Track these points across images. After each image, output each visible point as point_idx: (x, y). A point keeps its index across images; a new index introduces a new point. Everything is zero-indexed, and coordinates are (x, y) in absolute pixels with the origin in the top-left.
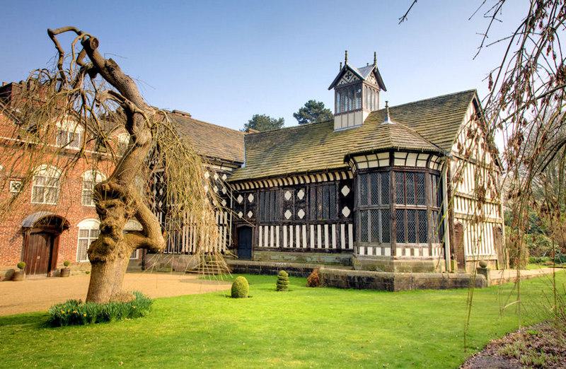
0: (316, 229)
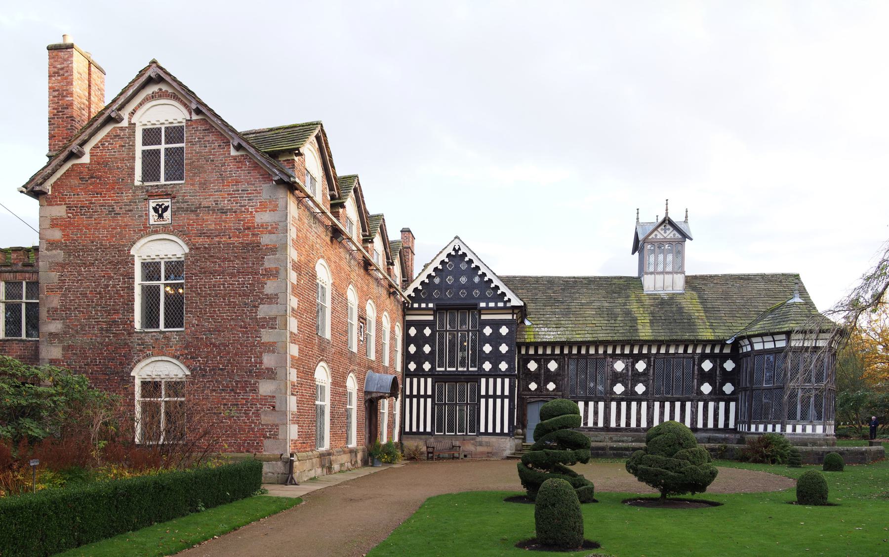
0: (662, 407)
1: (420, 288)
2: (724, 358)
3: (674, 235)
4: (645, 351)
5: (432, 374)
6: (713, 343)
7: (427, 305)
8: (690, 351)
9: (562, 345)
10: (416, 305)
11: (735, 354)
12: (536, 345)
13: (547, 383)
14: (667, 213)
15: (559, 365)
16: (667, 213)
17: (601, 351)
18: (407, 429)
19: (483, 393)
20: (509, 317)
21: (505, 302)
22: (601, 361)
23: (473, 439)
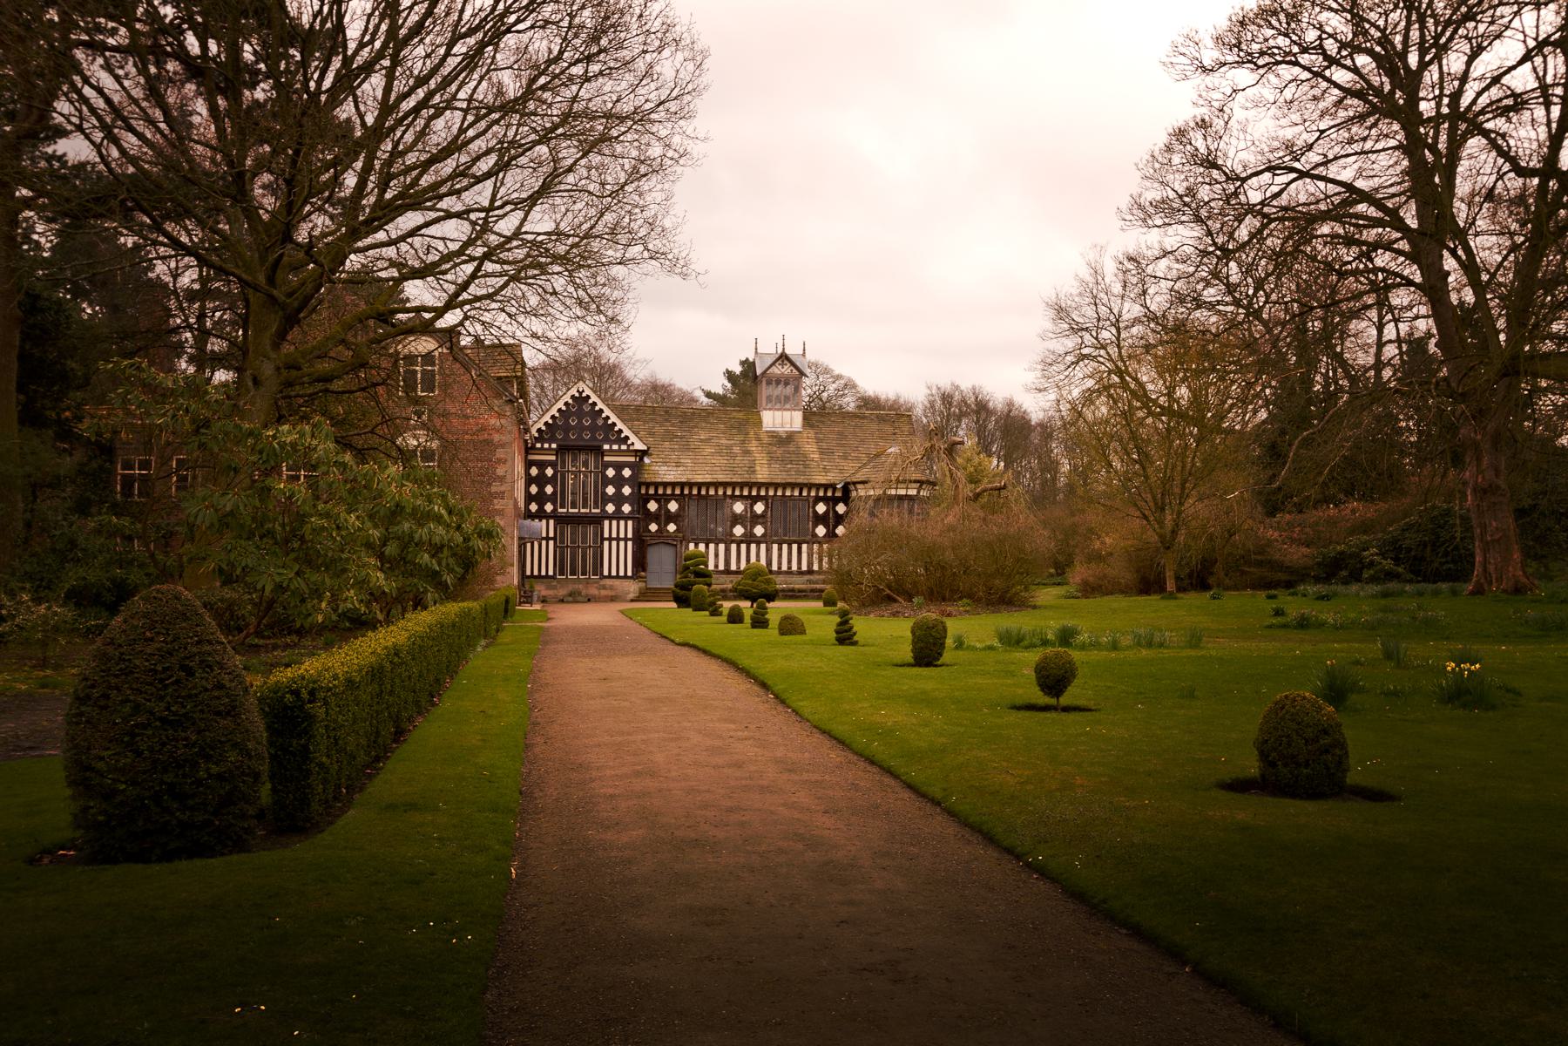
0: (780, 549)
12: (656, 485)
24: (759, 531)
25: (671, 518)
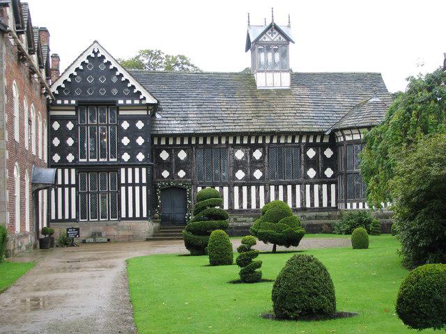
1: (63, 86)
2: (324, 147)
3: (280, 38)
4: (260, 141)
5: (75, 165)
6: (315, 134)
7: (70, 102)
8: (297, 141)
9: (190, 136)
10: (59, 102)
11: (333, 144)
12: (167, 137)
13: (177, 171)
14: (273, 20)
15: (188, 154)
16: (273, 20)
17: (223, 142)
18: (53, 217)
19: (123, 181)
20: (144, 113)
21: (141, 100)
22: (223, 151)
23: (114, 224)
24: (258, 174)
25: (180, 165)
